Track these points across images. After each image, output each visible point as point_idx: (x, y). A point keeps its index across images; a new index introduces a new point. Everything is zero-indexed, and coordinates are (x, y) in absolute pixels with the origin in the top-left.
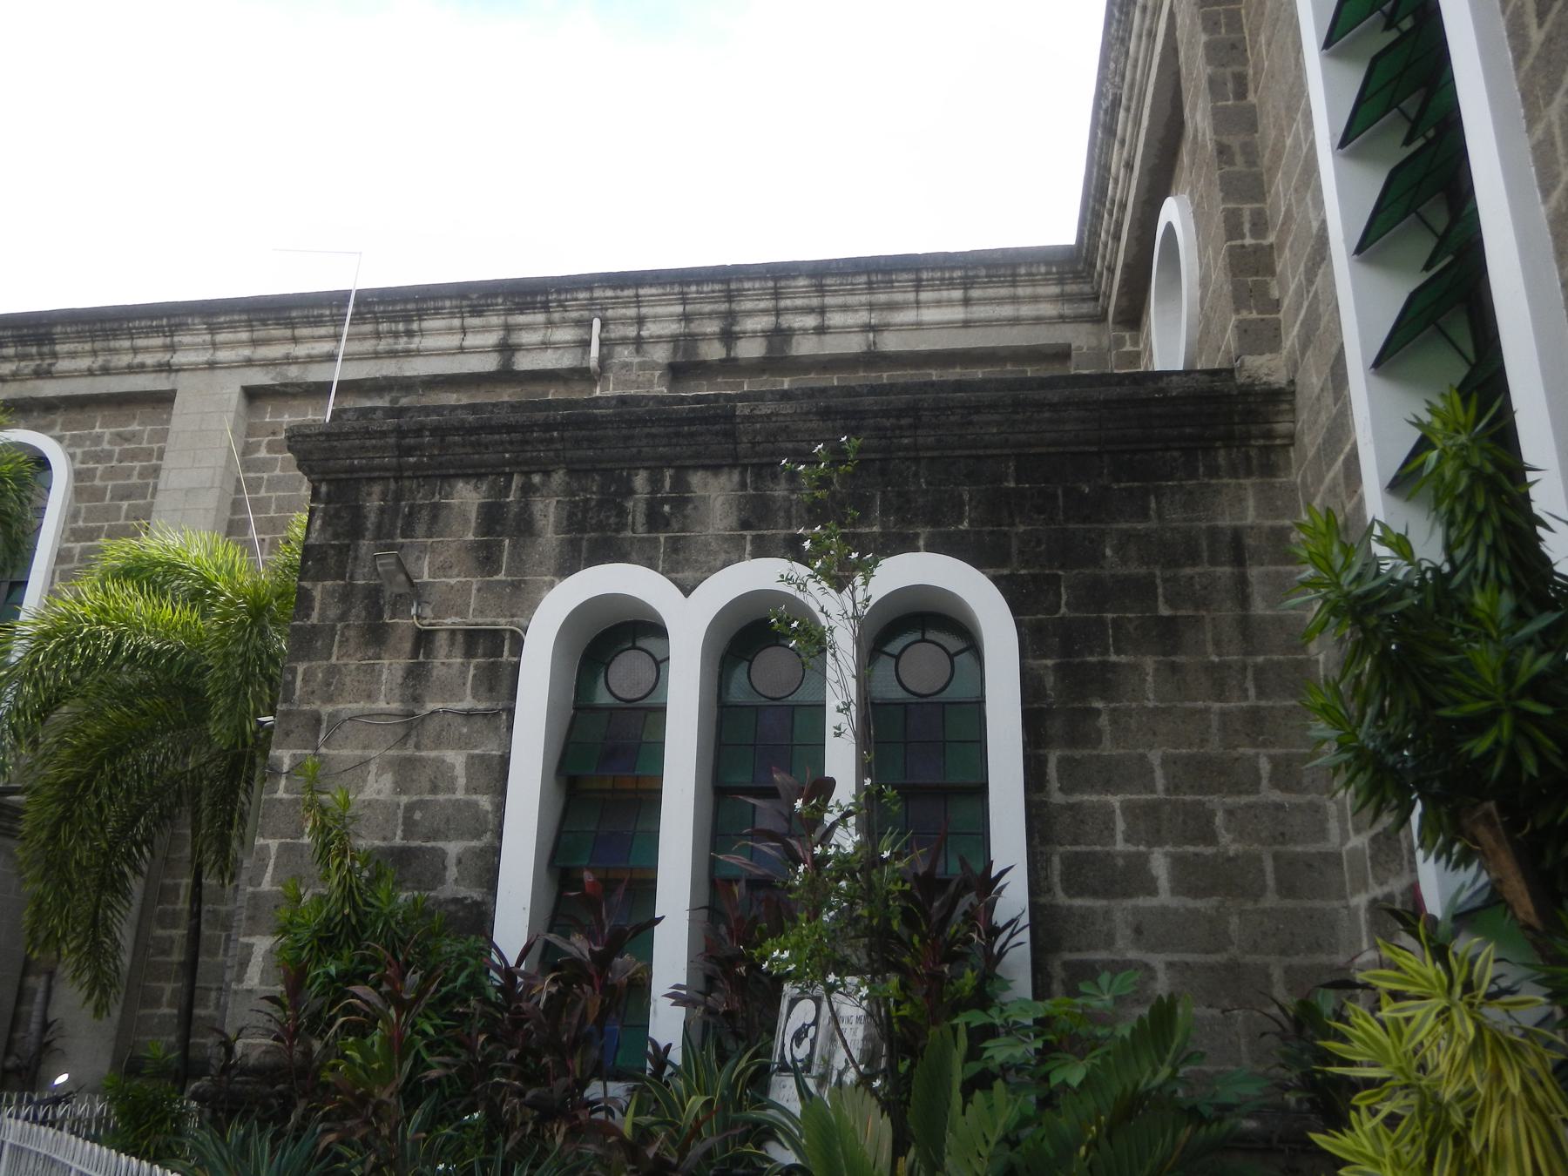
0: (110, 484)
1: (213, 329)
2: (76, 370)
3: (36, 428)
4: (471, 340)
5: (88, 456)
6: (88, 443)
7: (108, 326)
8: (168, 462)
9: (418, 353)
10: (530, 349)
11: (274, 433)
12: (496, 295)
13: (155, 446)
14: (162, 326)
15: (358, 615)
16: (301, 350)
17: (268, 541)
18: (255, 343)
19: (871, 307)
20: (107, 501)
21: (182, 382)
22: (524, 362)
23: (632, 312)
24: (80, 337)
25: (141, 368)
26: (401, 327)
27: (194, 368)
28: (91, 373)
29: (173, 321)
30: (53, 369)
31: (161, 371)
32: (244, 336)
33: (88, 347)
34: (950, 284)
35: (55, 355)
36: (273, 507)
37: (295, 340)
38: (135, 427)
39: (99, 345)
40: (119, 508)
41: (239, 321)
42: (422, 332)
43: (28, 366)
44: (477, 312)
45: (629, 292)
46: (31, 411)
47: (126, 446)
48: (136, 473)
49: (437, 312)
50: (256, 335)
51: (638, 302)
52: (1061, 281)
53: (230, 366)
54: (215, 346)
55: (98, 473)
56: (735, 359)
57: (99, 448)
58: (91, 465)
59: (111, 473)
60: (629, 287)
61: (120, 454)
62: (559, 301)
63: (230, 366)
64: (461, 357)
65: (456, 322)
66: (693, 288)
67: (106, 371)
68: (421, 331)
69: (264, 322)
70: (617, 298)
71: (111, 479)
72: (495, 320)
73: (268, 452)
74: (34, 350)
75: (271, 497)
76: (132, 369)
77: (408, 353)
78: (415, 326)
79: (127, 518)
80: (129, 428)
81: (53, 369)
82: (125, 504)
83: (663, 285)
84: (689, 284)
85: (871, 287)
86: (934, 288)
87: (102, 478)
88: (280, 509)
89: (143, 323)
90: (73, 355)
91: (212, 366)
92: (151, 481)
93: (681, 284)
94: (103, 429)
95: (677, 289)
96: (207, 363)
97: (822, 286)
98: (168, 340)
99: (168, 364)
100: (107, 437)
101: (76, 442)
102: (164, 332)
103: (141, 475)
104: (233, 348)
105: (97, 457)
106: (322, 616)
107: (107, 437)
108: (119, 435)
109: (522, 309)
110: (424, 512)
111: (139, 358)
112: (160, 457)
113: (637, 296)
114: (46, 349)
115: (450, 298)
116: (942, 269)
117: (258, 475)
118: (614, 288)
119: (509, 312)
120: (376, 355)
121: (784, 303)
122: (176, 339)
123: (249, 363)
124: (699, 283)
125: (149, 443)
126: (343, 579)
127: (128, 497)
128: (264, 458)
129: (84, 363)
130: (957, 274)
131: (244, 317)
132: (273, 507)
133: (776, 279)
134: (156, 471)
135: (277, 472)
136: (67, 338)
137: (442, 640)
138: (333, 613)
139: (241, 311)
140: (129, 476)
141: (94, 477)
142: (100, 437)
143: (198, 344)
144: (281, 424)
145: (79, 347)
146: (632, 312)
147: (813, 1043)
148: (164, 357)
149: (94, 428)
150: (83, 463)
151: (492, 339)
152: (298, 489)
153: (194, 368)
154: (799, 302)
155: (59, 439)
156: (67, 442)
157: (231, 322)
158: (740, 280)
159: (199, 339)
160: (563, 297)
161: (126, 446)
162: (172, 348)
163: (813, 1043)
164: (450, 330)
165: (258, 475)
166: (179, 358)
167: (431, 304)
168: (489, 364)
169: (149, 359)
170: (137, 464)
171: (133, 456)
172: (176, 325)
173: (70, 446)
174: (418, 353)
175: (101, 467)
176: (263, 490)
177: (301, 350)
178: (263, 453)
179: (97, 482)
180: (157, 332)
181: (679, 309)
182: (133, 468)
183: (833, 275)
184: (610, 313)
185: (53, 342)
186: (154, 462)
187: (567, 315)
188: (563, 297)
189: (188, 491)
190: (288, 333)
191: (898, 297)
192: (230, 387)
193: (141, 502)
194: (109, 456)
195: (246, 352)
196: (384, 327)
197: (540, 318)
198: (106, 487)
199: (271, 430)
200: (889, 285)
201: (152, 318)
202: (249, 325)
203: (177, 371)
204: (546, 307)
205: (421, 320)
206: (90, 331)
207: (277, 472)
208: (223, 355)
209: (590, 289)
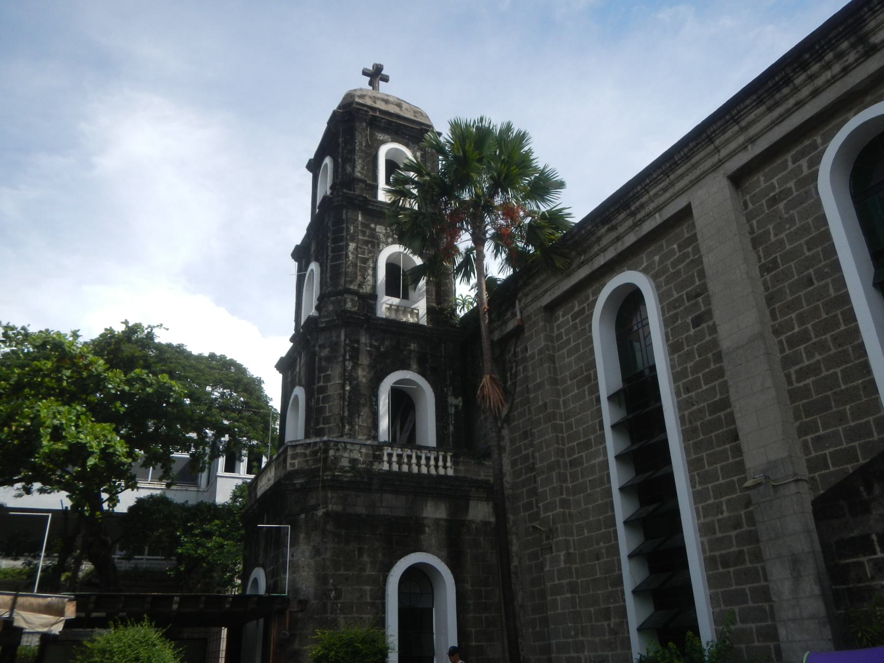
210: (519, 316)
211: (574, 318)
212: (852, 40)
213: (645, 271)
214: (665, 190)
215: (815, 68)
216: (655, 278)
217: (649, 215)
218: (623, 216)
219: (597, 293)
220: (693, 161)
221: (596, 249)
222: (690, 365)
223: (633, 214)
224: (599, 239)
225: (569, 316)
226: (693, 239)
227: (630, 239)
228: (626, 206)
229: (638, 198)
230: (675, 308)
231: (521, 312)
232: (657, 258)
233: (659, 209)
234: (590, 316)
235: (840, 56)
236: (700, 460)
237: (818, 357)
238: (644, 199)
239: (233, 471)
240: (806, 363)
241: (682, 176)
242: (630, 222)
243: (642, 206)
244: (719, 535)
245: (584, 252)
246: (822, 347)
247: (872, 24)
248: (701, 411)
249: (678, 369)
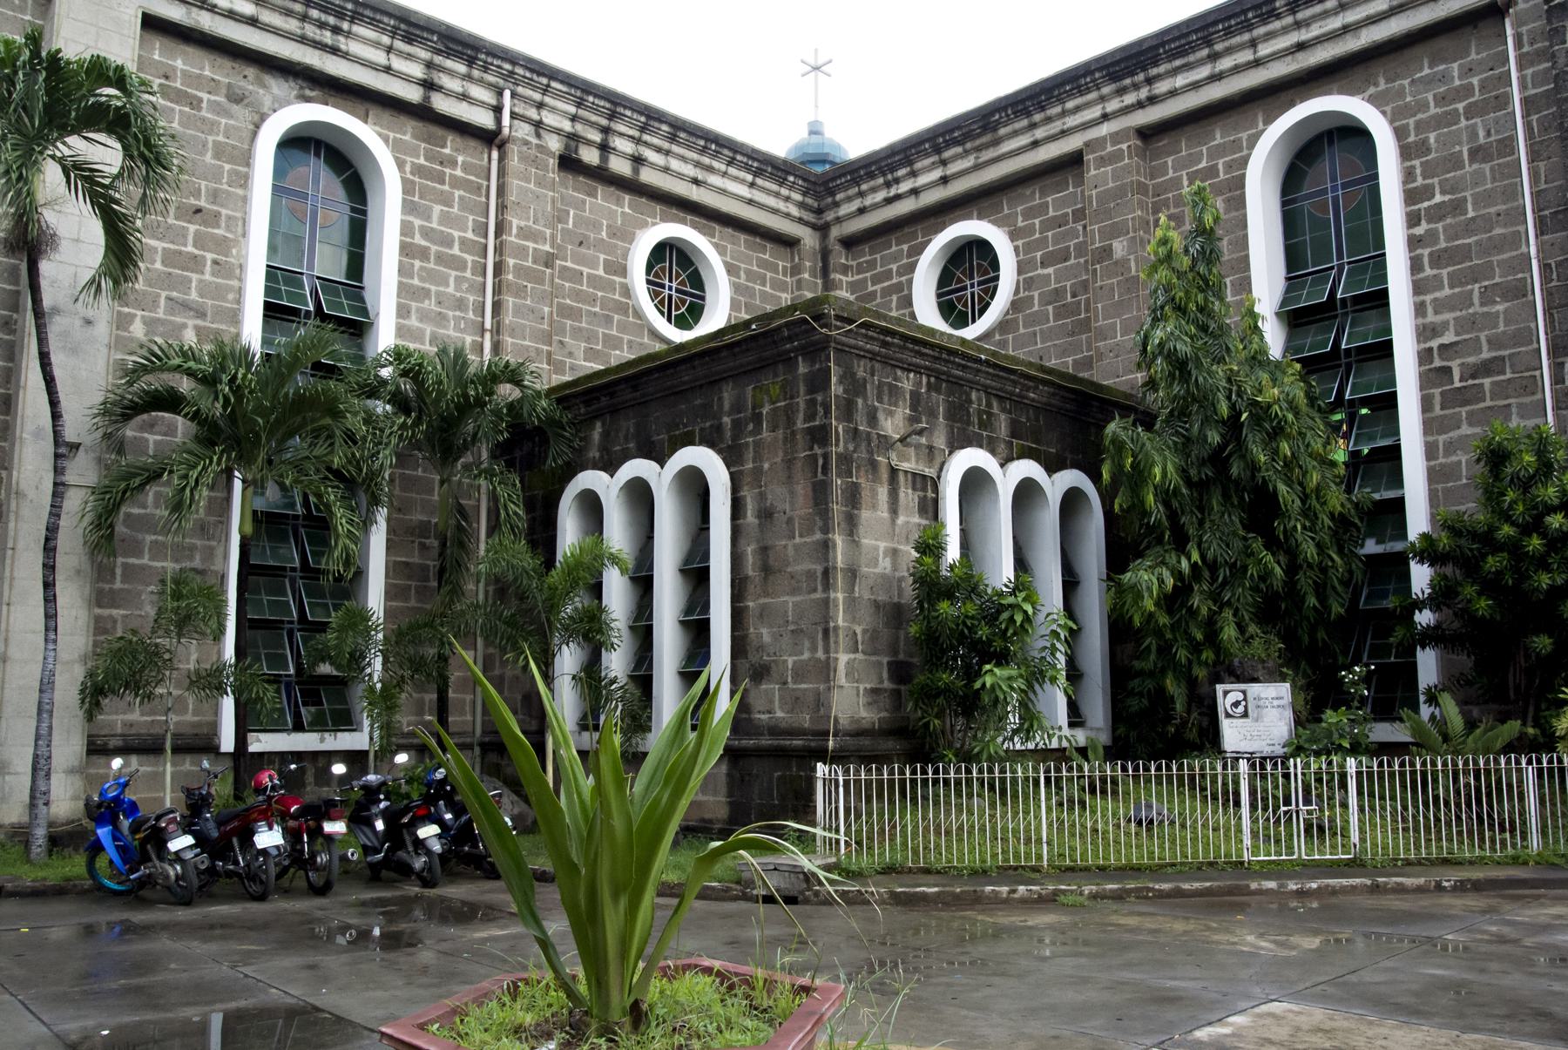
4: (398, 64)
9: (345, 55)
10: (449, 94)
12: (433, 32)
19: (698, 164)
22: (441, 104)
23: (537, 96)
26: (332, 20)
34: (747, 168)
42: (348, 35)
44: (409, 39)
45: (545, 81)
49: (373, 23)
51: (546, 90)
52: (804, 194)
56: (606, 170)
60: (544, 75)
62: (485, 62)
64: (384, 75)
65: (386, 40)
66: (591, 99)
68: (349, 32)
70: (531, 80)
72: (424, 54)
77: (334, 51)
78: (345, 26)
83: (570, 85)
84: (589, 93)
85: (703, 150)
86: (740, 168)
93: (583, 91)
95: (579, 93)
97: (675, 136)
109: (448, 54)
113: (548, 86)
115: (390, 15)
116: (749, 157)
118: (532, 71)
119: (438, 52)
120: (303, 40)
121: (646, 137)
124: (596, 96)
130: (755, 164)
133: (649, 117)
137: (901, 477)
146: (537, 96)
147: (1246, 707)
151: (417, 71)
154: (655, 141)
158: (625, 107)
160: (490, 60)
163: (1246, 707)
164: (376, 44)
167: (368, 12)
168: (413, 94)
174: (345, 55)
181: (572, 109)
183: (685, 131)
184: (520, 90)
187: (485, 76)
188: (490, 60)
191: (716, 164)
196: (315, 13)
197: (462, 68)
199: (162, 73)
200: (716, 155)
204: (471, 62)
205: (352, 22)
209: (514, 63)
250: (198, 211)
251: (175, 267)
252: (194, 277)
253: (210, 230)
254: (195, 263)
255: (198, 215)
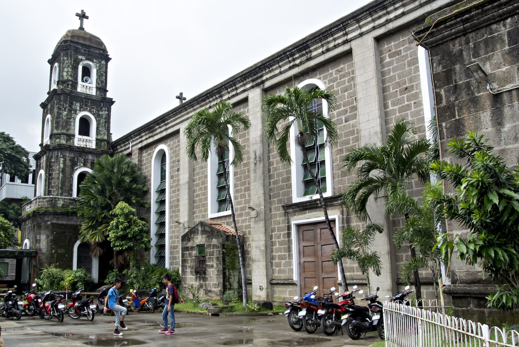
0: (339, 88)
1: (358, 22)
2: (318, 54)
3: (312, 78)
5: (330, 81)
6: (329, 77)
7: (324, 35)
8: (357, 73)
11: (390, 51)
13: (350, 70)
14: (341, 27)
15: (464, 97)
16: (392, 16)
17: (398, 91)
18: (374, 20)
20: (340, 94)
21: (353, 44)
24: (316, 43)
25: (338, 45)
27: (355, 38)
28: (323, 53)
29: (344, 24)
30: (312, 56)
31: (345, 43)
32: (370, 19)
33: (320, 44)
35: (311, 52)
36: (397, 78)
37: (388, 13)
38: (342, 66)
39: (323, 42)
40: (345, 95)
41: (366, 14)
43: (304, 58)
46: (309, 72)
47: (341, 74)
48: (346, 82)
50: (374, 17)
53: (368, 32)
54: (360, 27)
55: (335, 86)
57: (332, 77)
58: (332, 84)
59: (339, 84)
61: (340, 77)
63: (368, 32)
67: (328, 50)
69: (376, 12)
71: (339, 86)
73: (390, 58)
74: (304, 52)
75: (395, 75)
76: (335, 47)
79: (348, 98)
80: (340, 67)
81: (312, 56)
82: (346, 93)
87: (336, 87)
88: (400, 78)
89: (335, 29)
90: (316, 49)
91: (361, 35)
92: (352, 83)
94: (332, 71)
96: (359, 34)
98: (344, 32)
99: (347, 40)
100: (334, 73)
101: (325, 78)
102: (342, 29)
103: (348, 82)
104: (367, 25)
105: (333, 81)
106: (448, 101)
107: (334, 73)
108: (337, 71)
110: (482, 45)
111: (337, 42)
112: (353, 73)
114: (307, 51)
117: (388, 68)
122: (347, 30)
123: (374, 28)
125: (348, 70)
126: (452, 84)
127: (345, 92)
128: (389, 61)
129: (320, 51)
131: (368, 12)
132: (397, 78)
134: (353, 79)
135: (395, 65)
136: (313, 44)
138: (452, 99)
139: (366, 11)
140: (345, 84)
141: (334, 87)
142: (332, 73)
143: (354, 29)
144: (391, 46)
145: (317, 46)
148: (345, 38)
149: (329, 71)
150: (329, 84)
152: (404, 68)
153: (355, 38)
155: (320, 79)
156: (322, 79)
157: (364, 16)
159: (354, 27)
161: (341, 74)
162: (346, 34)
165: (388, 68)
166: (350, 36)
169: (340, 41)
170: (346, 78)
171: (344, 76)
172: (345, 25)
173: (323, 80)
175: (335, 83)
176: (392, 73)
177: (392, 16)
178: (388, 60)
179: (335, 89)
180: (340, 30)
182: (345, 80)
185: (309, 47)
186: (351, 76)
189: (366, 81)
190: (385, 12)
192: (369, 39)
193: (351, 91)
194: (336, 79)
195: (371, 25)
198: (338, 90)
199: (388, 50)
201: (337, 26)
202: (371, 15)
203: (350, 41)
206: (319, 39)
207: (395, 65)
208: (364, 29)
210: (130, 149)
211: (148, 155)
212: (219, 95)
213: (169, 146)
214: (175, 120)
215: (211, 99)
216: (171, 149)
217: (170, 128)
218: (163, 124)
219: (155, 148)
220: (182, 114)
221: (155, 133)
222: (174, 184)
223: (166, 125)
224: (156, 130)
225: (147, 154)
226: (179, 141)
227: (164, 134)
228: (164, 122)
229: (167, 120)
230: (174, 163)
231: (132, 147)
232: (172, 143)
233: (173, 126)
234: (152, 156)
235: (217, 98)
236: (173, 216)
237: (200, 192)
238: (169, 121)
239: (14, 182)
240: (198, 193)
241: (179, 118)
242: (164, 128)
243: (168, 123)
244: (174, 240)
245: (152, 132)
246: (201, 189)
247: (223, 93)
248: (175, 200)
249: (172, 185)
250: (406, 88)
251: (402, 112)
252: (409, 112)
253: (411, 93)
254: (409, 107)
255: (407, 90)
